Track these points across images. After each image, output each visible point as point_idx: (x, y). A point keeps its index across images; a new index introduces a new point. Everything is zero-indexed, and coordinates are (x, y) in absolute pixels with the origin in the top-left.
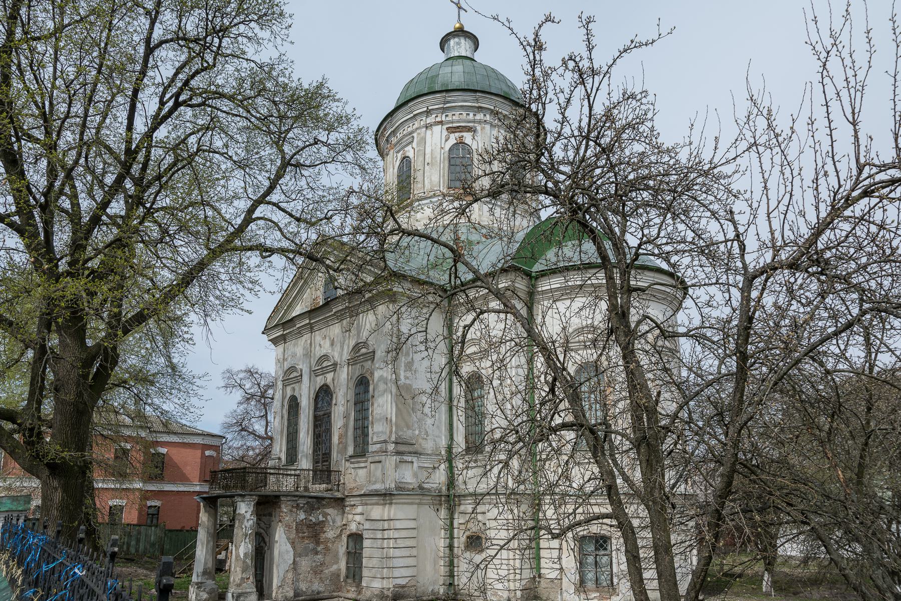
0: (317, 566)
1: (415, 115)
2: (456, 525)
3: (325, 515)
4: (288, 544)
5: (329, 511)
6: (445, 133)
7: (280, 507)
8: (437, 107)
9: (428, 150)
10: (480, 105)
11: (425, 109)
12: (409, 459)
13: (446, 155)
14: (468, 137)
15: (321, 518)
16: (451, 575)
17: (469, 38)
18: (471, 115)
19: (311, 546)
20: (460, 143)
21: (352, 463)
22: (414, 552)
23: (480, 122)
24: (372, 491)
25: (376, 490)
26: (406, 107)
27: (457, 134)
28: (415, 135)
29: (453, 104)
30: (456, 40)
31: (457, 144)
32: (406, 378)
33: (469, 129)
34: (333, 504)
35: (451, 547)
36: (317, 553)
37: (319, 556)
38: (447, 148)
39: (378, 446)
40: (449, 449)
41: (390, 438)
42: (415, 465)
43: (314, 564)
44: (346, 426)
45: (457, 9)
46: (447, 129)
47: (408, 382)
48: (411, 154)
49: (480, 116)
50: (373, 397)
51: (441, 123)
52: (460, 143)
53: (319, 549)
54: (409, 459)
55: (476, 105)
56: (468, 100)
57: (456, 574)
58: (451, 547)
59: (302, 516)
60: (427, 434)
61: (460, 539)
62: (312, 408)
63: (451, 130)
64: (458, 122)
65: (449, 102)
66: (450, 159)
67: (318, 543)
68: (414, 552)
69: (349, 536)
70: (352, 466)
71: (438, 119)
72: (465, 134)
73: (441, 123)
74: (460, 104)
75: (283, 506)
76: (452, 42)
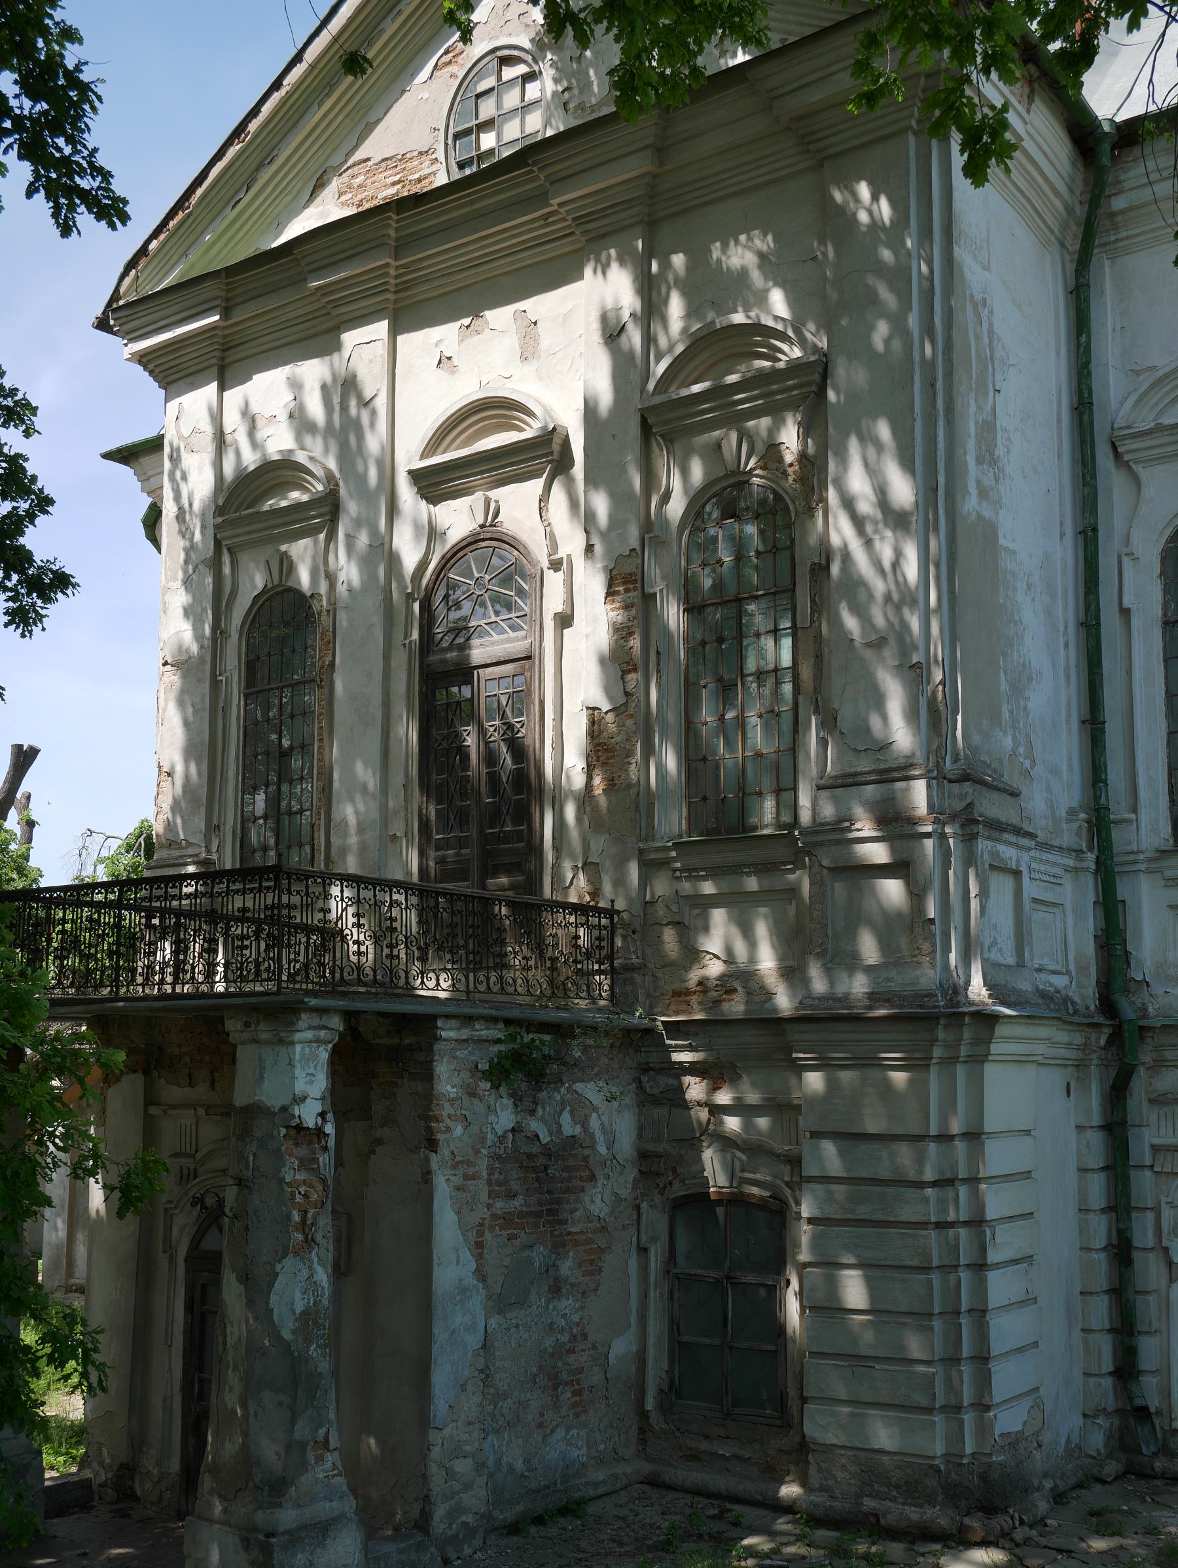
3: (581, 1109)
5: (591, 1091)
7: (427, 1075)
12: (1008, 853)
15: (569, 1127)
16: (1126, 1370)
32: (983, 493)
36: (556, 1290)
37: (566, 1304)
40: (1099, 823)
47: (987, 513)
53: (566, 1267)
54: (1008, 853)
59: (505, 1118)
67: (559, 1247)
75: (442, 1069)
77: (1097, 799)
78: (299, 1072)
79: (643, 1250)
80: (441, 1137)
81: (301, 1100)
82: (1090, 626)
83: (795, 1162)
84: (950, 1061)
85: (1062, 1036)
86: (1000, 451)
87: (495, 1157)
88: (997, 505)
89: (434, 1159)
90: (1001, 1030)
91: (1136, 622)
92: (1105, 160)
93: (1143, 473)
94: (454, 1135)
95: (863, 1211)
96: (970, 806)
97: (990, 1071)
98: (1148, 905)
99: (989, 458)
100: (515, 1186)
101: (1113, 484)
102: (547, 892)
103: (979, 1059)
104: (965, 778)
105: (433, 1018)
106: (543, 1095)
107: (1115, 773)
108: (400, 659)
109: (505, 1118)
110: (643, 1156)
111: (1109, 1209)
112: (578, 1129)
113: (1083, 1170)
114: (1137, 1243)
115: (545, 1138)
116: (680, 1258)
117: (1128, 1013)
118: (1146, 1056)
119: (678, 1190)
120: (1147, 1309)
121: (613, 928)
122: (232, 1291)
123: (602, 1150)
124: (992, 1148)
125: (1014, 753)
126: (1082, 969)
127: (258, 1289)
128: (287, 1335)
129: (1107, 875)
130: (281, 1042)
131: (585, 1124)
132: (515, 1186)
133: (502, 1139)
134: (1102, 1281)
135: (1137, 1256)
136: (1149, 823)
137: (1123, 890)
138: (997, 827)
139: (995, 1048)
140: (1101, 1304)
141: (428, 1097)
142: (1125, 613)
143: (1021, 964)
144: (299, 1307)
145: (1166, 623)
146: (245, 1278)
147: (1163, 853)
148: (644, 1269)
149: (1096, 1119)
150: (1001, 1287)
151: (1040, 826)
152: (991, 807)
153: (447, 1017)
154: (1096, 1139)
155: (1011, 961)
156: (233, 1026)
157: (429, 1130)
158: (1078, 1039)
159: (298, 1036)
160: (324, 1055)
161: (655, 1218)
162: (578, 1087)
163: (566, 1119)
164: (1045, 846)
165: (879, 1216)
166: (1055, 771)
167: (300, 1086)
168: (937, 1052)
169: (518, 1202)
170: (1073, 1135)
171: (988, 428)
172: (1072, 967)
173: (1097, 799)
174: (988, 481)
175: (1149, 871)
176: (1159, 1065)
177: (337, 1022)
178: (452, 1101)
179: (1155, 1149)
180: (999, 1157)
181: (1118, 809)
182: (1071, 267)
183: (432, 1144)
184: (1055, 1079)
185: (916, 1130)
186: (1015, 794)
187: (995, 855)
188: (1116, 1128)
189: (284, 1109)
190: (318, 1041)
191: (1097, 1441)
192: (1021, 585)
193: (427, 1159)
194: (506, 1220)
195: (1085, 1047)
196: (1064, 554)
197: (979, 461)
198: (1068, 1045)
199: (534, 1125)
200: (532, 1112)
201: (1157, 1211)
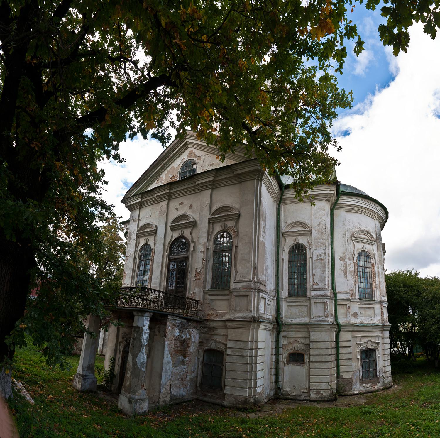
2: (281, 345)
3: (190, 334)
5: (191, 330)
7: (166, 324)
12: (264, 296)
15: (188, 336)
19: (181, 358)
21: (210, 295)
24: (238, 318)
25: (242, 318)
32: (263, 237)
34: (195, 325)
35: (277, 362)
37: (185, 367)
39: (244, 284)
40: (277, 292)
41: (254, 278)
42: (267, 302)
44: (205, 267)
50: (237, 247)
54: (264, 296)
60: (268, 280)
61: (284, 354)
62: (167, 253)
67: (185, 356)
69: (205, 351)
70: (210, 297)
75: (168, 323)
77: (277, 288)
78: (145, 321)
79: (198, 358)
80: (167, 335)
81: (144, 326)
82: (277, 261)
83: (226, 345)
84: (253, 328)
85: (270, 326)
86: (266, 231)
87: (175, 340)
88: (265, 240)
89: (166, 339)
90: (262, 324)
91: (284, 261)
92: (283, 190)
93: (286, 238)
94: (169, 334)
95: (237, 354)
96: (259, 287)
97: (259, 331)
98: (284, 306)
99: (264, 232)
100: (178, 345)
101: (282, 239)
102: (187, 296)
103: (258, 328)
104: (258, 282)
105: (168, 315)
106: (184, 330)
107: (280, 284)
108: (165, 256)
109: (177, 334)
110: (200, 342)
111: (275, 355)
112: (189, 337)
113: (272, 348)
114: (279, 360)
115: (184, 337)
116: (205, 360)
117: (280, 322)
119: (205, 348)
120: (280, 371)
121: (198, 304)
122: (130, 358)
124: (259, 343)
125: (265, 280)
126: (273, 316)
127: (135, 356)
128: (139, 366)
129: (278, 300)
130: (142, 316)
131: (191, 336)
132: (178, 345)
133: (177, 337)
134: (274, 367)
135: (279, 362)
136: (285, 293)
137: (280, 303)
138: (262, 291)
139: (260, 327)
140: (273, 370)
141: (166, 328)
142: (283, 259)
143: (265, 313)
144: (141, 361)
146: (133, 355)
147: (287, 297)
148: (198, 362)
149: (274, 340)
150: (259, 367)
151: (269, 291)
152: (262, 287)
153: (170, 315)
154: (274, 342)
155: (263, 313)
156: (135, 313)
157: (165, 334)
159: (145, 315)
160: (149, 319)
161: (201, 353)
162: (190, 329)
163: (188, 335)
164: (269, 295)
165: (240, 355)
166: (271, 283)
167: (145, 324)
168: (251, 327)
171: (264, 227)
173: (277, 288)
174: (264, 235)
175: (284, 300)
176: (284, 331)
177: (152, 314)
178: (169, 329)
180: (260, 345)
181: (280, 290)
182: (277, 205)
183: (165, 336)
186: (266, 286)
187: (262, 295)
188: (277, 341)
189: (142, 327)
190: (148, 317)
192: (268, 253)
193: (164, 339)
195: (273, 328)
196: (274, 249)
197: (263, 232)
199: (182, 335)
200: (182, 333)
201: (283, 355)
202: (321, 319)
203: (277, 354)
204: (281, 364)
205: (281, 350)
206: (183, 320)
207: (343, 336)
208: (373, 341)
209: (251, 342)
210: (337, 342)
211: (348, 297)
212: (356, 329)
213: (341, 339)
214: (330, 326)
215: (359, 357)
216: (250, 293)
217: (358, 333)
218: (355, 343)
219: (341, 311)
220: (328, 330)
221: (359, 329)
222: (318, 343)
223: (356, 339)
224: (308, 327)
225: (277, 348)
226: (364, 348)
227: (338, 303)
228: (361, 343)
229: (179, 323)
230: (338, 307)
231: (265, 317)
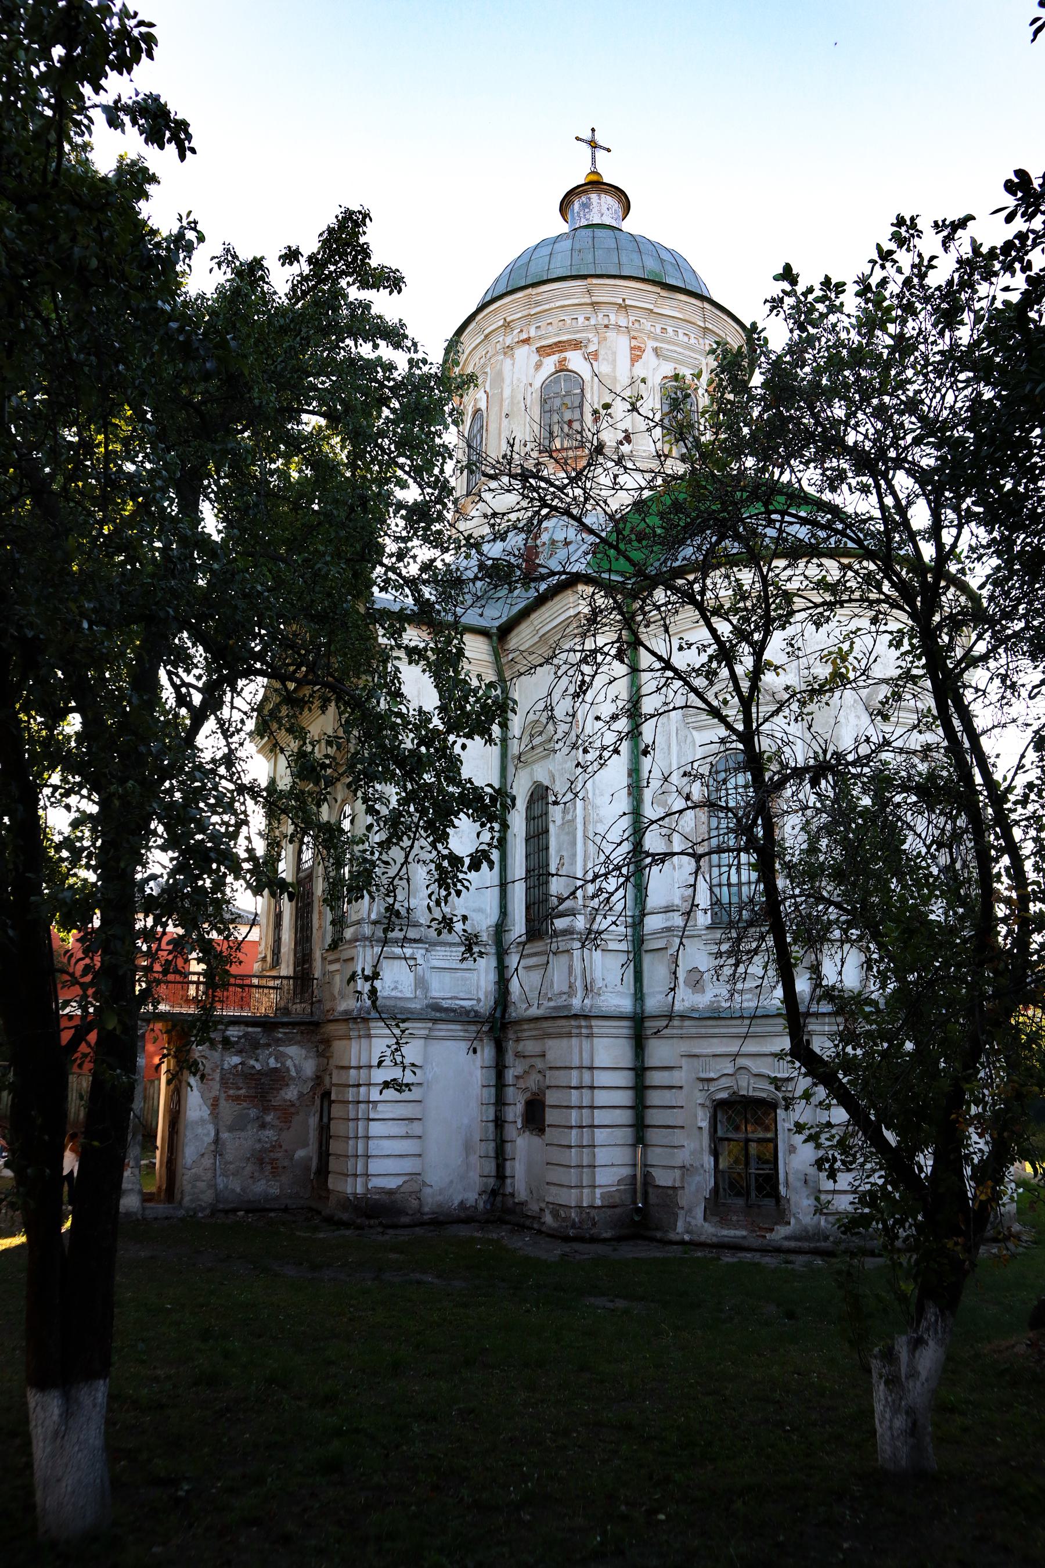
0: (263, 1150)
1: (486, 336)
2: (510, 1075)
3: (280, 1057)
4: (204, 1108)
5: (292, 1051)
6: (535, 358)
8: (519, 315)
9: (507, 393)
10: (595, 299)
11: (501, 323)
13: (536, 396)
14: (576, 361)
16: (501, 1175)
17: (606, 192)
18: (581, 319)
20: (562, 368)
22: (416, 1128)
23: (596, 327)
26: (473, 325)
27: (555, 358)
28: (488, 370)
29: (547, 307)
30: (584, 199)
31: (557, 372)
33: (576, 345)
35: (499, 1122)
36: (263, 1126)
38: (537, 384)
43: (258, 1146)
45: (587, 150)
46: (538, 350)
48: (483, 405)
49: (600, 319)
51: (526, 341)
52: (562, 368)
55: (588, 301)
56: (574, 292)
57: (508, 1173)
58: (499, 1122)
63: (544, 351)
64: (557, 335)
65: (538, 304)
66: (544, 401)
68: (416, 1128)
71: (524, 336)
72: (569, 355)
73: (526, 341)
74: (558, 304)
76: (576, 206)
84: (360, 1037)
85: (459, 1027)
90: (372, 1024)
103: (369, 1036)
110: (318, 1077)
115: (258, 1066)
118: (511, 1035)
123: (293, 1073)
129: (501, 954)
133: (236, 1066)
145: (527, 840)
158: (473, 1028)
169: (242, 1092)
170: (478, 1073)
172: (482, 997)
179: (517, 1077)
184: (464, 1046)
185: (346, 1064)
188: (499, 1068)
191: (481, 1205)
194: (237, 1098)
195: (478, 1032)
198: (466, 1031)
199: (252, 1062)
202: (561, 1001)
203: (500, 1102)
204: (511, 1132)
205: (510, 1093)
206: (250, 1029)
207: (659, 1052)
208: (755, 1070)
209: (359, 1068)
210: (640, 1070)
211: (668, 924)
212: (694, 1031)
213: (650, 1062)
214: (573, 1023)
215: (705, 1124)
216: (354, 951)
217: (704, 1042)
218: (694, 1076)
219: (656, 971)
220: (569, 1035)
221: (703, 1031)
222: (557, 1073)
223: (695, 1060)
224: (539, 1025)
225: (500, 1085)
226: (724, 1095)
227: (649, 945)
228: (712, 1075)
229: (239, 1037)
230: (647, 960)
231: (416, 1005)
